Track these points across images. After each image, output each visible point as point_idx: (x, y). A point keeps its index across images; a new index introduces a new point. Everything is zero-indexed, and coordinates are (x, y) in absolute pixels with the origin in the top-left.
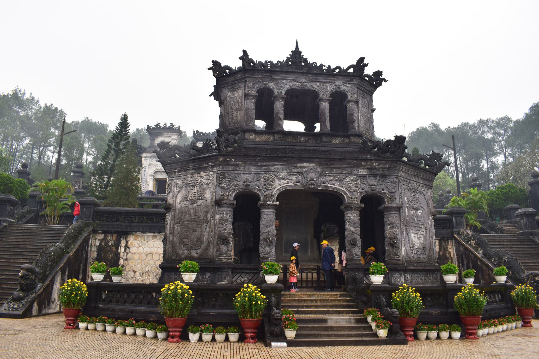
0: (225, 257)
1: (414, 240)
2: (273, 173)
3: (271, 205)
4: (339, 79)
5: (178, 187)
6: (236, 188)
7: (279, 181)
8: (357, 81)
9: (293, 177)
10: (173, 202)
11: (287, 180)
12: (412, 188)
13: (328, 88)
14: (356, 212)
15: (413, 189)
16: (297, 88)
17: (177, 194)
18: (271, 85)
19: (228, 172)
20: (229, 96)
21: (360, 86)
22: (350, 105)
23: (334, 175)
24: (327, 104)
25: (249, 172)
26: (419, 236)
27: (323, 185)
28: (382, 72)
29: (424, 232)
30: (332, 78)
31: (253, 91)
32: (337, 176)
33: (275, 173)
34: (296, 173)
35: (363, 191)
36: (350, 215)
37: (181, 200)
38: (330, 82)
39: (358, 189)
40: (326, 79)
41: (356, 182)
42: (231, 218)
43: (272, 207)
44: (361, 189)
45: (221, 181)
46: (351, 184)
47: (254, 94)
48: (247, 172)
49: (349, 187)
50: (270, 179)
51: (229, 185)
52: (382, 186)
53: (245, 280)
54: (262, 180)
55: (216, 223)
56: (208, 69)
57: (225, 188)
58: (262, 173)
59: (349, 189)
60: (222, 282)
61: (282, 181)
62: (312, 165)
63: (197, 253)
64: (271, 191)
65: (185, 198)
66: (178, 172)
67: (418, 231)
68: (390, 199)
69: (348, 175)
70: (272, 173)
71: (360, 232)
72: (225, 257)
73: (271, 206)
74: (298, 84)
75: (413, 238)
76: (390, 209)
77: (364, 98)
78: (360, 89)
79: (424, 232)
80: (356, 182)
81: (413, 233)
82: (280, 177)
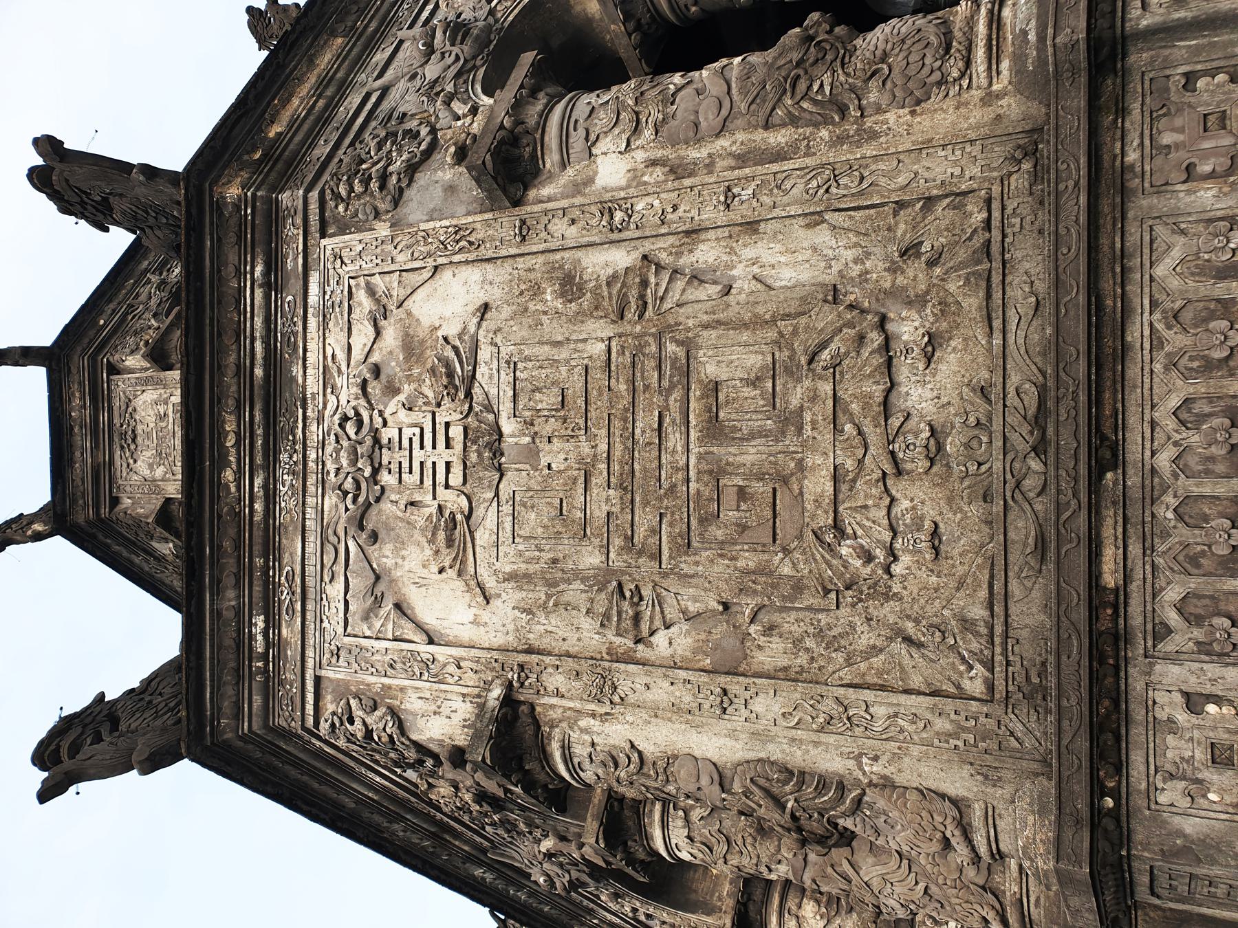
5: (366, 618)
10: (470, 679)
17: (419, 626)
20: (151, 466)
37: (459, 584)
45: (366, 182)
55: (659, 172)
63: (932, 344)
65: (450, 542)
66: (272, 622)
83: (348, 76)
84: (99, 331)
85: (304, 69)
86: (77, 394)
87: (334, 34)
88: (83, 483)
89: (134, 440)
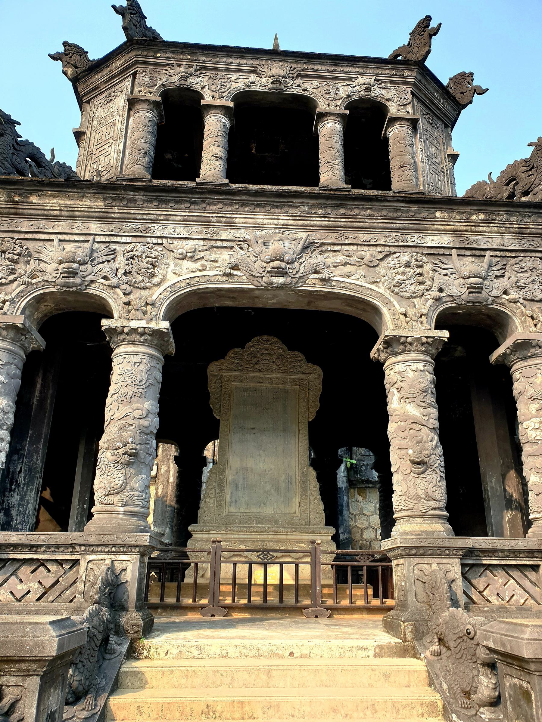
2: (160, 241)
3: (140, 330)
4: (368, 71)
6: (34, 281)
7: (176, 265)
8: (410, 74)
9: (221, 254)
11: (203, 262)
13: (341, 91)
14: (421, 357)
16: (262, 89)
19: (16, 236)
21: (420, 90)
23: (349, 248)
24: (338, 126)
25: (82, 238)
27: (317, 276)
28: (471, 74)
30: (350, 69)
31: (151, 93)
32: (358, 251)
33: (164, 241)
34: (229, 244)
35: (443, 295)
36: (398, 368)
38: (344, 79)
39: (428, 290)
41: (418, 271)
42: (8, 375)
44: (435, 288)
46: (403, 273)
48: (77, 238)
49: (398, 285)
50: (146, 257)
51: (13, 272)
52: (503, 283)
53: (29, 592)
54: (121, 260)
58: (124, 240)
59: (396, 290)
61: (187, 264)
68: (532, 318)
70: (155, 241)
71: (437, 424)
73: (142, 335)
74: (264, 80)
76: (533, 350)
77: (431, 124)
78: (418, 98)
80: (418, 271)
82: (180, 251)
83: (79, 217)
84: (153, 56)
85: (76, 196)
86: (121, 62)
87: (105, 199)
88: (91, 84)
89: (108, 102)
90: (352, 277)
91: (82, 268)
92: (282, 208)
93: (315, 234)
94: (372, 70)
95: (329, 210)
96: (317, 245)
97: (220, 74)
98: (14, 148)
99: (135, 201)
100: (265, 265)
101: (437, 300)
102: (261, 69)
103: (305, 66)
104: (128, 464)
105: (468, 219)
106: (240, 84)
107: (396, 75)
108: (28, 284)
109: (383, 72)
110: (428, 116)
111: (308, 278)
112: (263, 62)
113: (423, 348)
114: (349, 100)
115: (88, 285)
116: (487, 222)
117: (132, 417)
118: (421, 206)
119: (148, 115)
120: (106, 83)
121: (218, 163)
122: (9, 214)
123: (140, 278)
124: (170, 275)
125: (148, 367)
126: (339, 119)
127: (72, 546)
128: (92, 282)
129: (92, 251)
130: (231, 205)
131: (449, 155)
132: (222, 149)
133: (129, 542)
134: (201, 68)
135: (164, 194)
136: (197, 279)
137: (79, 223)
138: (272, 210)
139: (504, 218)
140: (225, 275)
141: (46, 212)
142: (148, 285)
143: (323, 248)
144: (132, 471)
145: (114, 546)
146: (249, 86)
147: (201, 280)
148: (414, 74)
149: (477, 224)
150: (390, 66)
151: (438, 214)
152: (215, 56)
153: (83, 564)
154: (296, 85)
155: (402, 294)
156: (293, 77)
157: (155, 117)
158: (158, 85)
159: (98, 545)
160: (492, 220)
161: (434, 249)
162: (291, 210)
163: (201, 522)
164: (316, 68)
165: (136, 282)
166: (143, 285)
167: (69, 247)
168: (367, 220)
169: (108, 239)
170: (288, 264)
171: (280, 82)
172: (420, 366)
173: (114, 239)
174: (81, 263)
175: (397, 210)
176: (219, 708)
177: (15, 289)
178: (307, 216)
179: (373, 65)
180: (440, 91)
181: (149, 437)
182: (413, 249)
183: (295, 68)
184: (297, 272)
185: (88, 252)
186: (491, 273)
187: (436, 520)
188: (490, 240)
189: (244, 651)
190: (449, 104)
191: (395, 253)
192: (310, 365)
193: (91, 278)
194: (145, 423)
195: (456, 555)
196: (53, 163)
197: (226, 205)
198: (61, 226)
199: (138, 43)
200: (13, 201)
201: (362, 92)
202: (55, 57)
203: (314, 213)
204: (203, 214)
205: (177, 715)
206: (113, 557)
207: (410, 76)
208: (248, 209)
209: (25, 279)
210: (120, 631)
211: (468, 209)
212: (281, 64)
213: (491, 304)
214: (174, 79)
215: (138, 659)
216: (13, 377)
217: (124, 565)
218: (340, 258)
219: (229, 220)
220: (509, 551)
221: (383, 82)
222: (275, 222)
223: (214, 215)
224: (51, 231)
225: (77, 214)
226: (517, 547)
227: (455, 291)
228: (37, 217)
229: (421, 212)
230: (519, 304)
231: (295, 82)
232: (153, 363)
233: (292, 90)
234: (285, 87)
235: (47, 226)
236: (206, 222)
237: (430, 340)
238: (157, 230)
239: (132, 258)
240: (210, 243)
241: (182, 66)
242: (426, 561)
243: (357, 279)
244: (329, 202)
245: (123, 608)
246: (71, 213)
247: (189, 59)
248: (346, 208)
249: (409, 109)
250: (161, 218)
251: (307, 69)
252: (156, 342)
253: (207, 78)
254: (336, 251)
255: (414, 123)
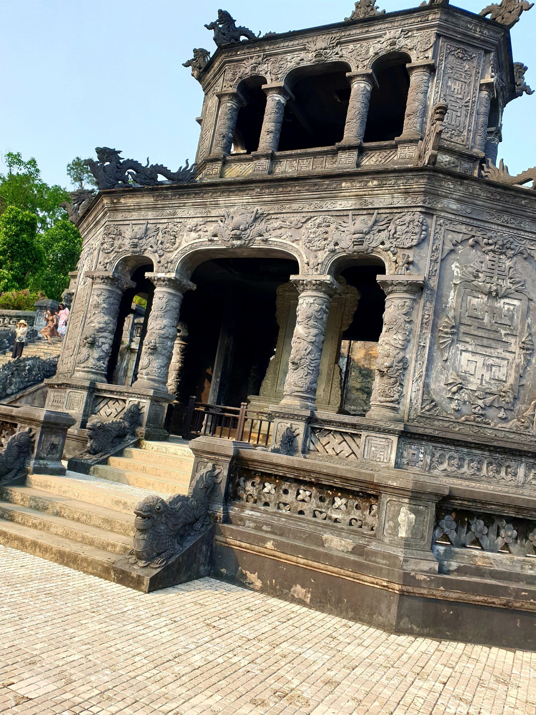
0: (84, 367)
1: (471, 368)
3: (162, 278)
4: (396, 24)
6: (120, 250)
8: (434, 17)
11: (199, 233)
12: (485, 241)
15: (488, 244)
16: (309, 64)
18: (263, 69)
19: (116, 223)
21: (447, 29)
22: (415, 78)
23: (285, 215)
26: (490, 362)
27: (260, 238)
29: (514, 353)
30: (379, 27)
31: (231, 86)
32: (290, 217)
35: (336, 247)
38: (376, 37)
40: (368, 31)
42: (109, 303)
43: (166, 285)
44: (332, 243)
47: (232, 91)
52: (383, 235)
56: (183, 65)
57: (106, 251)
58: (163, 221)
59: (308, 245)
60: (73, 409)
61: (193, 235)
62: (246, 199)
64: (169, 255)
67: (489, 350)
68: (396, 262)
69: (312, 214)
70: (178, 220)
72: (84, 367)
73: (164, 281)
74: (310, 55)
75: (464, 362)
76: (390, 288)
79: (514, 353)
81: (466, 351)
82: (188, 226)
87: (153, 197)
90: (282, 238)
91: (140, 241)
92: (245, 191)
93: (265, 207)
94: (399, 22)
95: (272, 190)
96: (265, 215)
97: (280, 57)
98: (118, 168)
99: (168, 196)
100: (230, 232)
101: (331, 252)
102: (309, 46)
103: (343, 34)
104: (151, 354)
105: (366, 185)
106: (293, 63)
107: (421, 21)
108: (118, 252)
109: (410, 22)
110: (459, 51)
111: (255, 240)
112: (311, 39)
113: (314, 288)
114: (377, 57)
115: (144, 251)
116: (380, 186)
117: (155, 329)
118: (331, 180)
119: (229, 104)
120: (213, 79)
121: (268, 137)
122: (112, 210)
123: (168, 245)
124: (183, 242)
125: (166, 300)
126: (364, 79)
127: (121, 393)
128: (145, 249)
129: (147, 230)
130: (216, 193)
131: (481, 85)
132: (273, 124)
133: (144, 393)
134: (268, 56)
135: (180, 190)
136: (195, 244)
137: (143, 213)
138: (239, 194)
139: (393, 182)
140: (210, 240)
141: (128, 208)
142: (172, 249)
143: (269, 217)
144: (153, 358)
145: (139, 394)
146: (298, 64)
147: (198, 245)
148: (438, 16)
149: (373, 188)
150: (415, 14)
151: (344, 184)
152: (276, 44)
153: (127, 402)
154: (335, 53)
155: (311, 248)
156: (333, 46)
157: (234, 104)
158: (237, 78)
159: (133, 393)
160: (384, 185)
161: (341, 212)
162: (251, 192)
163: (262, 394)
164: (352, 33)
165: (166, 249)
166: (168, 250)
167: (136, 228)
168: (296, 194)
169: (156, 221)
170: (243, 231)
171: (322, 54)
172: (311, 300)
173: (159, 221)
174: (140, 239)
175: (315, 185)
176: (147, 469)
177: (112, 255)
178: (260, 194)
179: (400, 18)
180: (475, 21)
181: (165, 340)
182: (326, 213)
183: (335, 38)
184: (249, 236)
185: (143, 231)
186: (375, 227)
187: (298, 399)
188: (383, 200)
189: (184, 453)
190: (489, 30)
191: (314, 217)
192: (349, 286)
193: (144, 247)
194: (162, 332)
195: (301, 420)
196: (149, 167)
197: (213, 193)
198: (135, 215)
199: (225, 47)
200: (114, 203)
201: (388, 47)
202: (186, 65)
203: (264, 193)
204: (202, 201)
205: (132, 469)
206: (139, 400)
207: (434, 19)
208: (226, 194)
209: (116, 250)
210: (134, 434)
211: (365, 178)
212: (324, 37)
213: (372, 253)
214: (248, 70)
215: (141, 448)
216: (113, 304)
217: (144, 405)
218: (277, 224)
219: (216, 202)
220: (340, 422)
221: (409, 31)
222: (242, 201)
223: (208, 200)
224: (130, 219)
225: (142, 207)
226: (344, 421)
227: (345, 244)
228: (124, 211)
229: (332, 184)
230: (389, 252)
231: (334, 50)
232: (171, 297)
233: (331, 59)
234: (325, 57)
235: (128, 215)
236: (204, 205)
237: (318, 282)
238: (180, 213)
239: (165, 233)
240: (206, 219)
241: (254, 58)
242: (285, 421)
243: (284, 239)
244: (272, 184)
245: (141, 425)
246: (139, 207)
247: (259, 51)
248: (283, 187)
249: (430, 54)
250: (182, 205)
251: (344, 36)
252: (172, 285)
253: (271, 62)
254: (277, 218)
255: (431, 69)
